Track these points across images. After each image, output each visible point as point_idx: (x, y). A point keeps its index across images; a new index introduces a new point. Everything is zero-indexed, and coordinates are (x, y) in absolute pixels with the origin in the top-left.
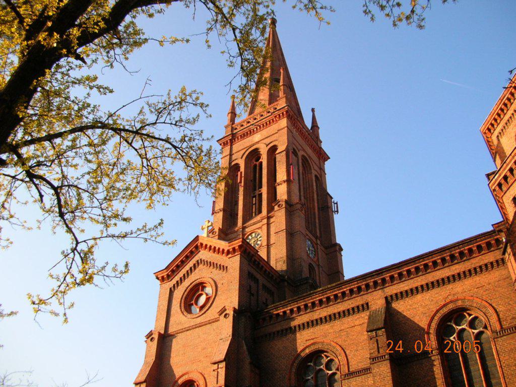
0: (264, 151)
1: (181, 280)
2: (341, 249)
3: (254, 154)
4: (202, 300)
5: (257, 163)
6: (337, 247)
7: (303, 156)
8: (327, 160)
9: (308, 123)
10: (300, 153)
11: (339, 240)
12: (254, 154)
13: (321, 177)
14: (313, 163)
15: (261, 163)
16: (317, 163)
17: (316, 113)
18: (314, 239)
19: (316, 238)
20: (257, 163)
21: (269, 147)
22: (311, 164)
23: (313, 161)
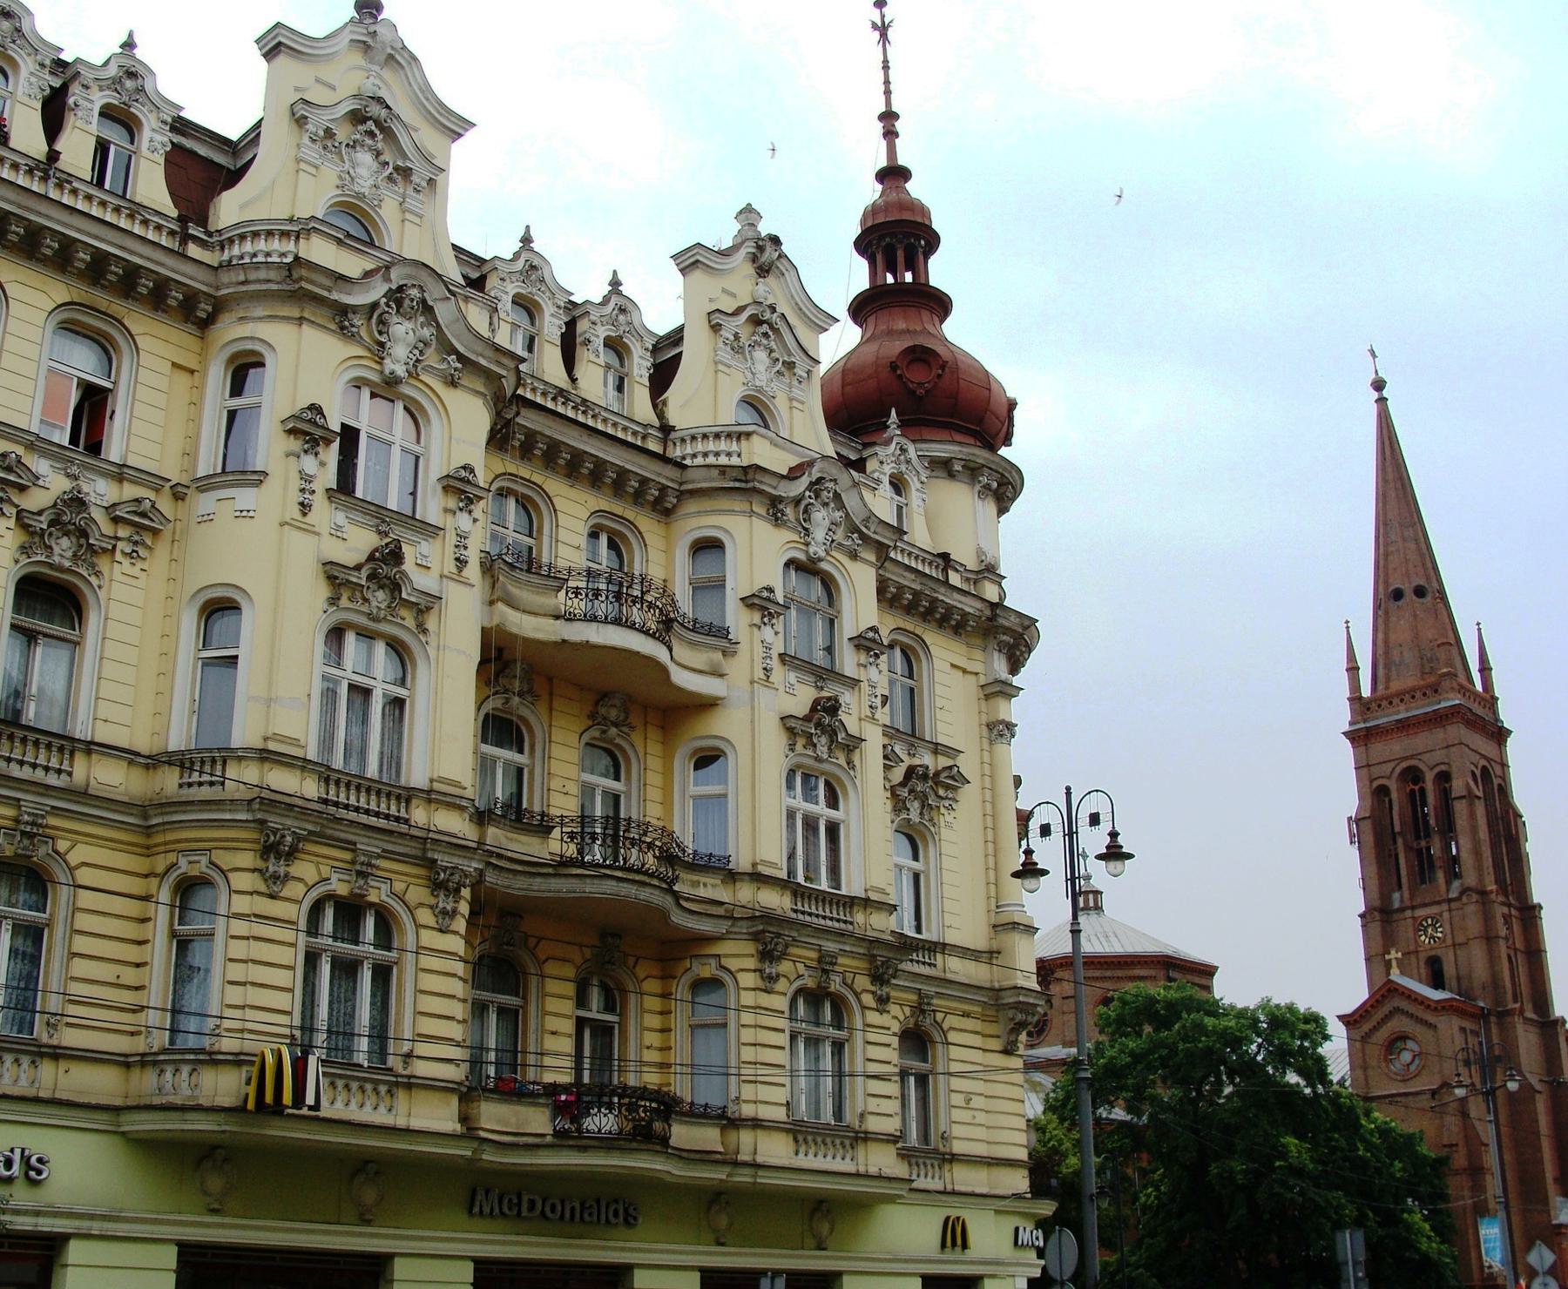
0: (1429, 777)
1: (1375, 1029)
2: (1541, 907)
3: (1412, 775)
4: (1406, 1057)
10: (1478, 773)
11: (1536, 897)
12: (1412, 775)
15: (1422, 790)
19: (1509, 905)
21: (1436, 770)
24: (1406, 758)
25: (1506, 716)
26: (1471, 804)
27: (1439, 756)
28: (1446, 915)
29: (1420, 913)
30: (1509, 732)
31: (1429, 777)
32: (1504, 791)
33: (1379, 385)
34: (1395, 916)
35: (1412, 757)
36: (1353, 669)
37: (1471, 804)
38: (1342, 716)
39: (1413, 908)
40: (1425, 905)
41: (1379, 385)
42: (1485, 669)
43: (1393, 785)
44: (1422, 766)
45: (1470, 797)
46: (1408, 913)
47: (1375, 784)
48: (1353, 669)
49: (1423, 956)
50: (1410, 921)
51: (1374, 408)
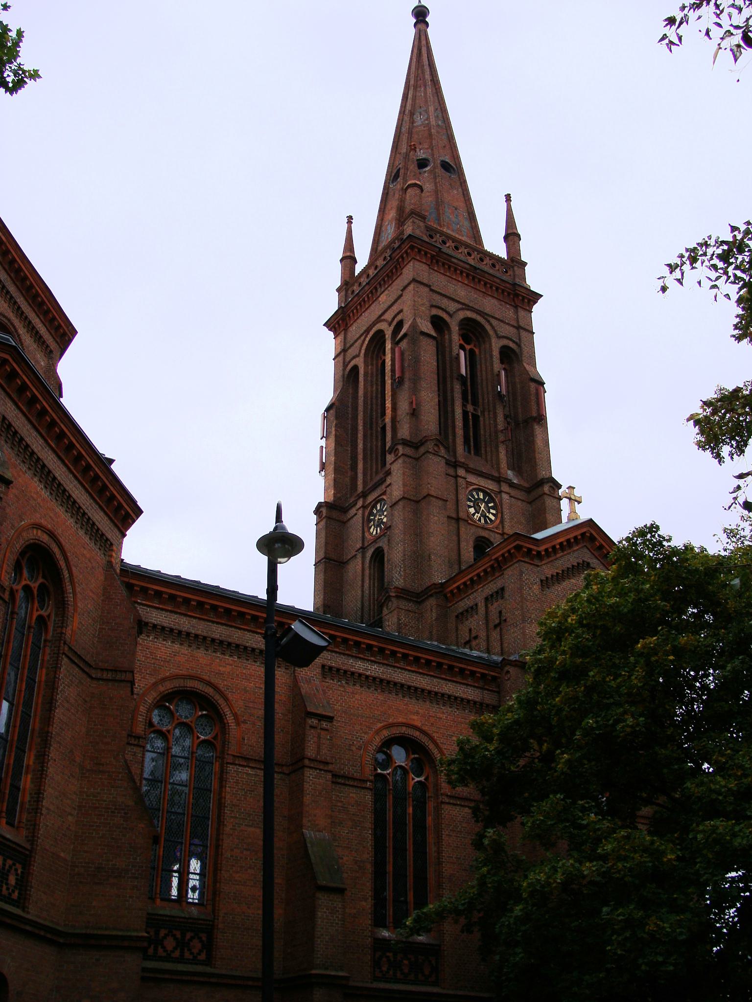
6: (546, 488)
13: (519, 346)
14: (493, 321)
18: (490, 485)
19: (498, 480)
21: (394, 323)
22: (488, 327)
25: (533, 280)
26: (414, 342)
27: (395, 309)
29: (370, 498)
30: (536, 297)
32: (517, 355)
34: (353, 511)
37: (414, 342)
39: (364, 495)
42: (512, 237)
43: (360, 362)
45: (416, 334)
46: (360, 503)
47: (349, 367)
48: (349, 259)
51: (412, 31)
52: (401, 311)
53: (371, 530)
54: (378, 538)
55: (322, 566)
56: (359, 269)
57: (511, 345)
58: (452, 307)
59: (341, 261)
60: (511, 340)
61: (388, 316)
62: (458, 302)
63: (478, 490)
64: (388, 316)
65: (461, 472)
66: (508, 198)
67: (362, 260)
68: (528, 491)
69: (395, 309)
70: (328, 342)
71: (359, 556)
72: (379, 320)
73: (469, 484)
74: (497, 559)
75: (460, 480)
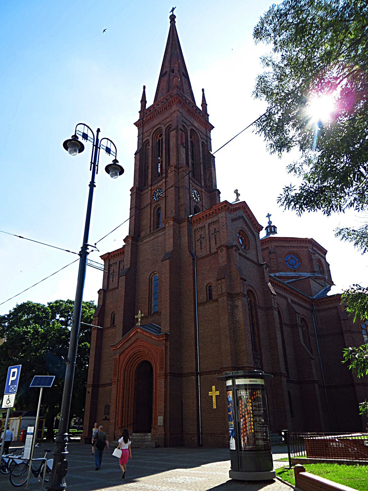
5: (160, 138)
6: (217, 192)
7: (192, 129)
8: (212, 129)
9: (199, 103)
10: (189, 129)
12: (158, 132)
14: (200, 133)
15: (162, 139)
16: (204, 132)
17: (205, 92)
19: (201, 187)
20: (160, 138)
21: (166, 126)
22: (198, 134)
23: (201, 132)
24: (157, 125)
25: (211, 120)
27: (168, 120)
28: (164, 184)
31: (164, 128)
33: (173, 18)
35: (157, 125)
36: (144, 101)
38: (137, 117)
39: (151, 186)
40: (156, 184)
41: (173, 18)
42: (204, 104)
43: (150, 138)
44: (162, 126)
46: (150, 189)
47: (144, 140)
48: (144, 101)
49: (153, 206)
50: (149, 192)
52: (171, 121)
53: (155, 198)
54: (157, 201)
55: (134, 210)
56: (148, 105)
57: (205, 142)
58: (188, 123)
59: (141, 101)
60: (204, 139)
61: (165, 122)
62: (191, 123)
63: (195, 190)
64: (165, 122)
65: (191, 181)
66: (203, 90)
67: (150, 102)
68: (210, 192)
69: (168, 120)
70: (136, 129)
71: (149, 207)
72: (159, 124)
73: (193, 186)
74: (215, 210)
75: (191, 184)
